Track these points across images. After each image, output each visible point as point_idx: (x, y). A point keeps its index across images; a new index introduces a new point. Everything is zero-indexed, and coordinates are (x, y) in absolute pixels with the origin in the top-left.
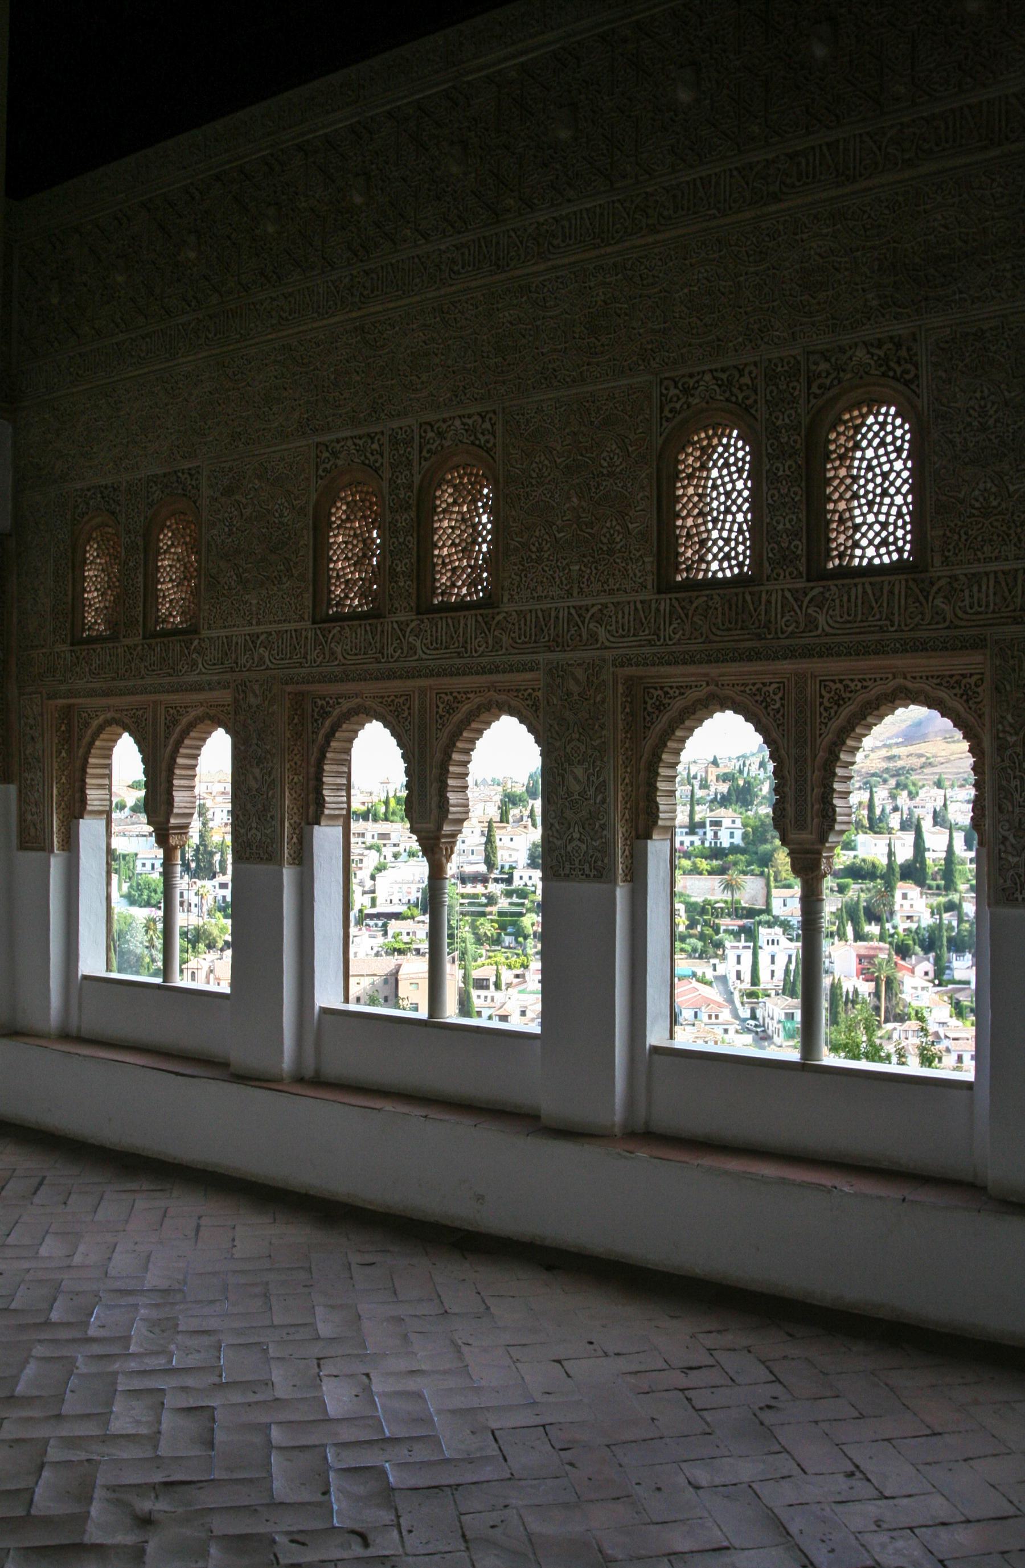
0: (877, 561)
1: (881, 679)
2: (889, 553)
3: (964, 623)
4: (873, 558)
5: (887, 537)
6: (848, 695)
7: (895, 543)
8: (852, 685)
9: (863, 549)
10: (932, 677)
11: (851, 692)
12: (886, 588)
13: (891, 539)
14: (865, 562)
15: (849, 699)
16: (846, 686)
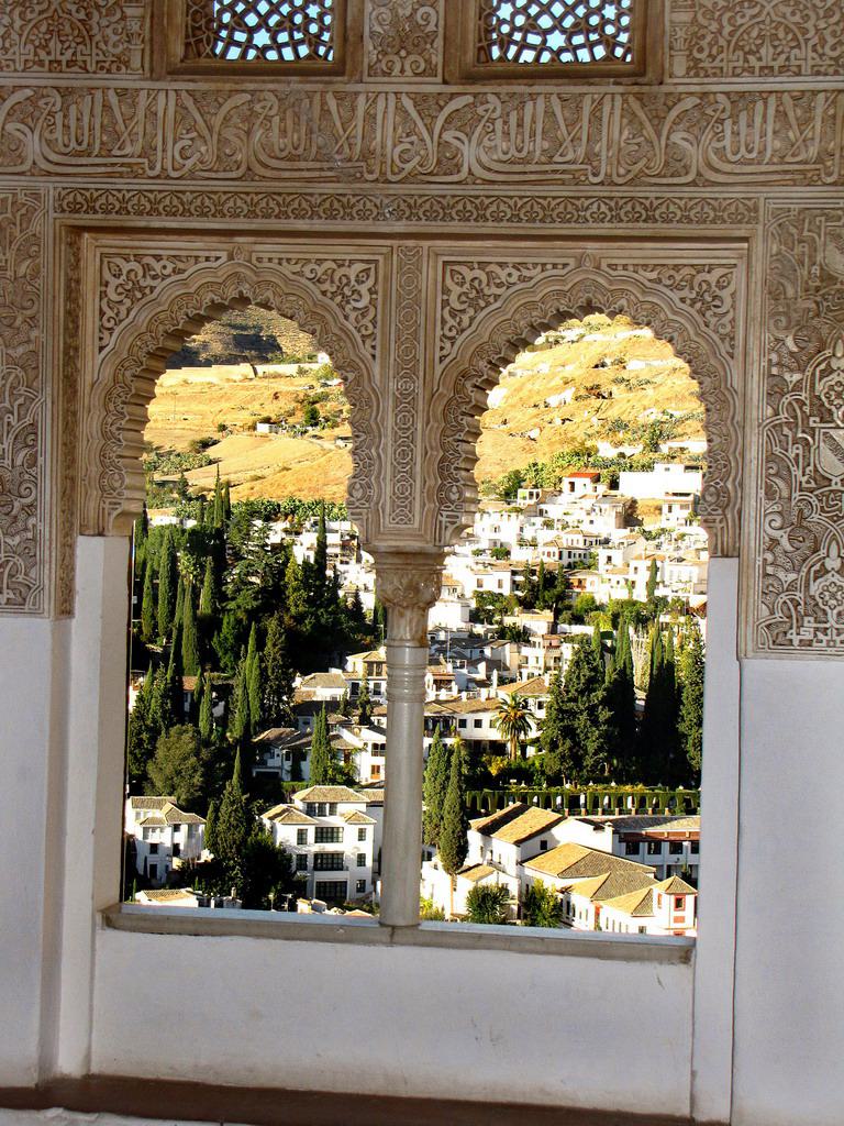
0: (272, 55)
1: (207, 259)
2: (295, 45)
3: (268, 173)
4: (266, 48)
5: (291, 15)
6: (149, 282)
7: (305, 28)
8: (157, 266)
9: (251, 31)
10: (288, 260)
11: (154, 277)
12: (143, 100)
13: (298, 19)
14: (252, 54)
15: (152, 289)
16: (147, 268)
